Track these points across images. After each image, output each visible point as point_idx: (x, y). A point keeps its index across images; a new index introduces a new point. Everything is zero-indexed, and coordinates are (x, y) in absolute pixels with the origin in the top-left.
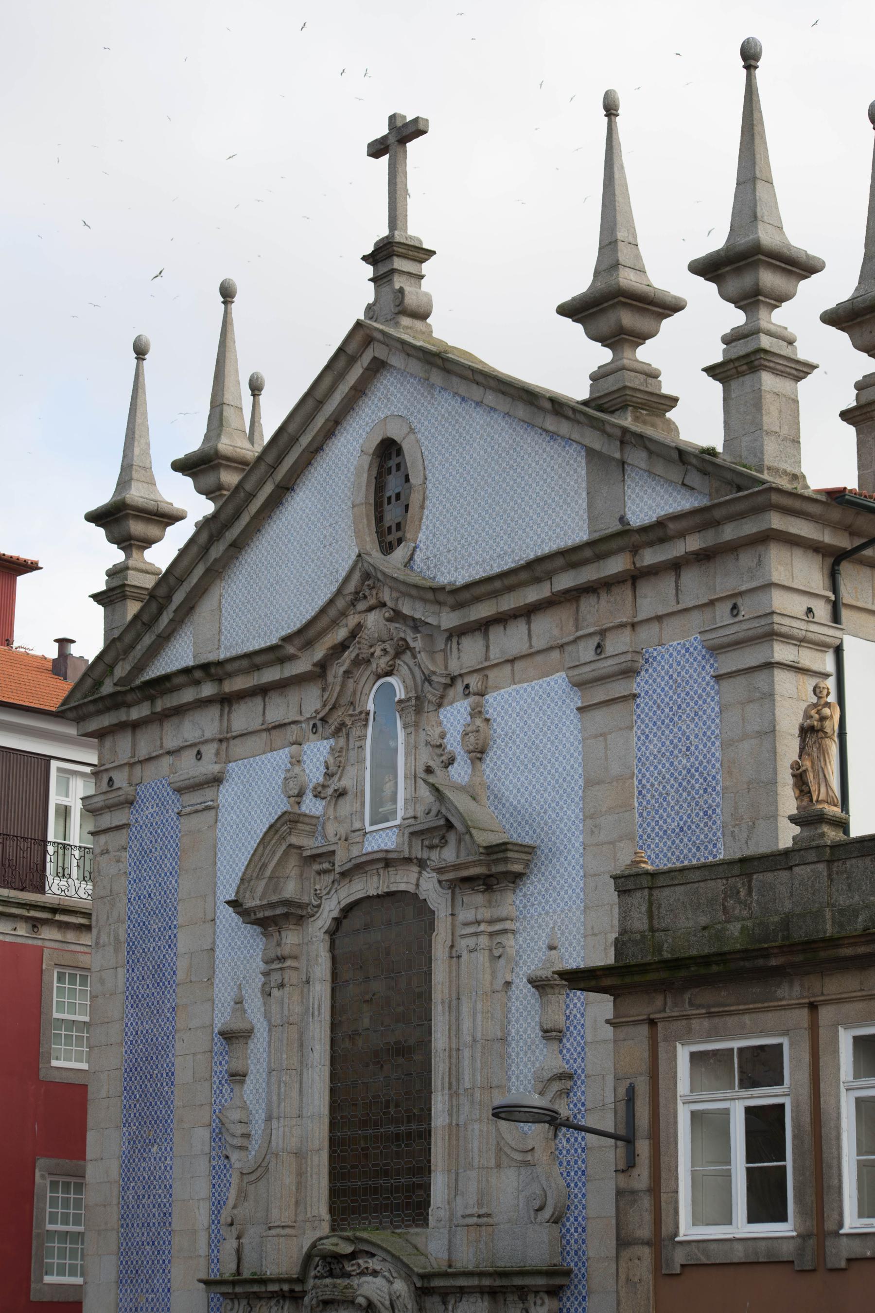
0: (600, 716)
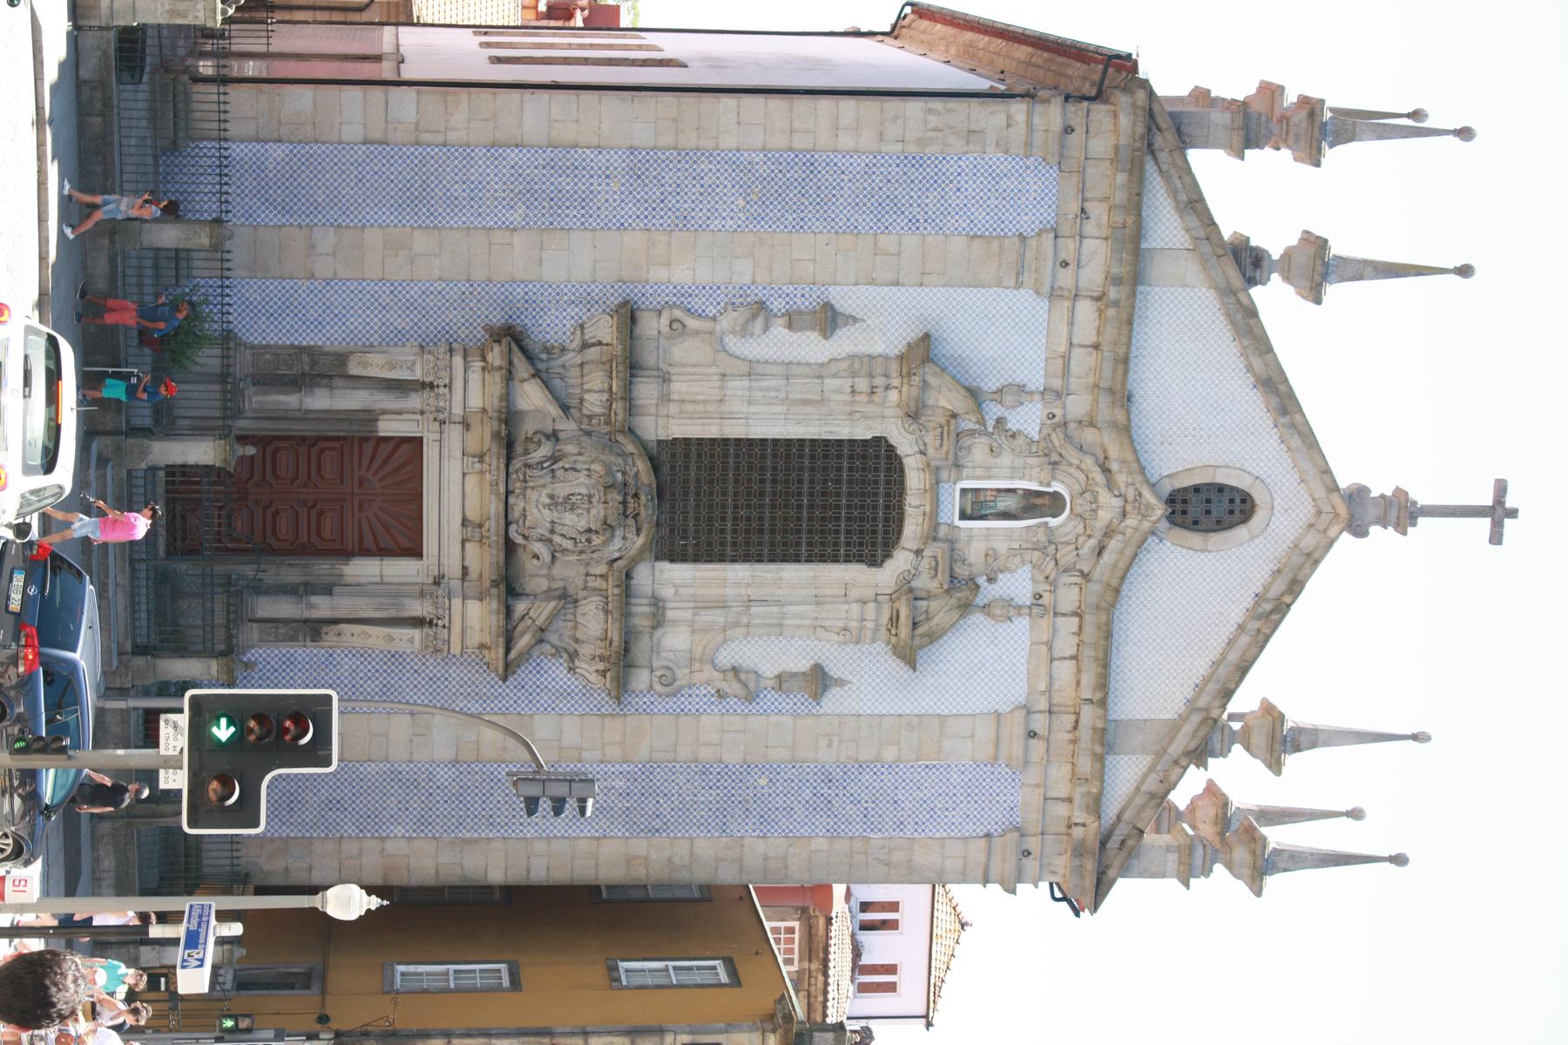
0: (985, 731)
